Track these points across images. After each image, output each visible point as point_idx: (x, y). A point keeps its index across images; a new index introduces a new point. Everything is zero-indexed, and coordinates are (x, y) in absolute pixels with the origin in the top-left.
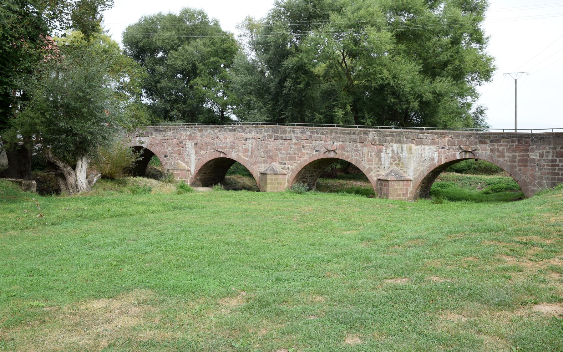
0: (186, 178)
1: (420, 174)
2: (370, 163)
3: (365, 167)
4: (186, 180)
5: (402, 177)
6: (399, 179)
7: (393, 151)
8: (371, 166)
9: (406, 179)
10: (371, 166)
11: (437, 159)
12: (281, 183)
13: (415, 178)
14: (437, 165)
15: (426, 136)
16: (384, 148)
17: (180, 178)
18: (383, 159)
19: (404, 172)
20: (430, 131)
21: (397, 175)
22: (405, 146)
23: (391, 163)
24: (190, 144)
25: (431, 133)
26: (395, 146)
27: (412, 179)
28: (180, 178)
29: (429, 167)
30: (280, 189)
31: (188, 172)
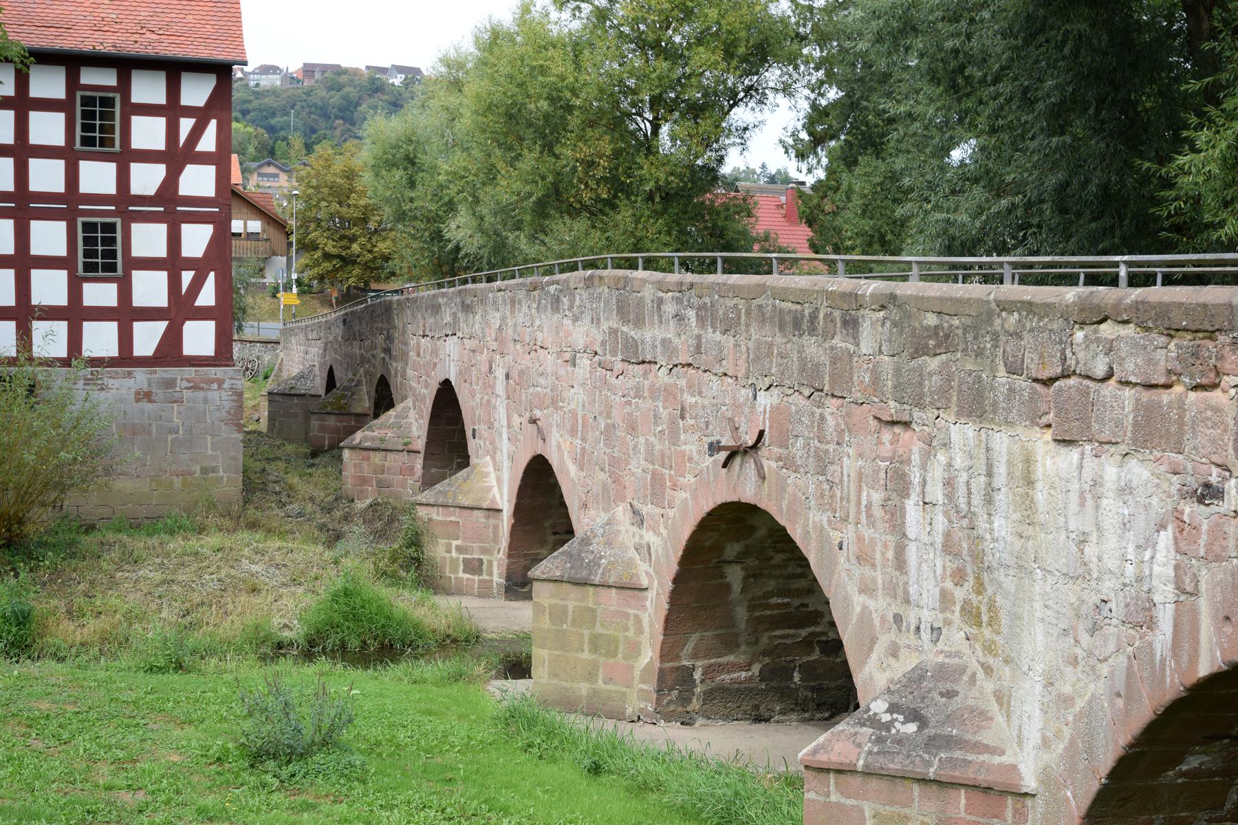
0: (484, 551)
1: (1072, 742)
2: (867, 571)
3: (847, 599)
4: (485, 558)
5: (950, 742)
6: (894, 766)
7: (949, 483)
8: (871, 604)
9: (970, 775)
10: (871, 604)
11: (1170, 608)
12: (615, 641)
13: (1046, 776)
14: (1173, 686)
15: (1110, 348)
16: (917, 448)
17: (459, 549)
18: (912, 552)
19: (999, 697)
20: (1158, 293)
21: (914, 716)
22: (1001, 441)
23: (946, 599)
24: (500, 373)
25: (1139, 317)
26: (962, 433)
27: (1030, 783)
28: (459, 549)
29: (1120, 686)
30: (608, 680)
31: (492, 521)
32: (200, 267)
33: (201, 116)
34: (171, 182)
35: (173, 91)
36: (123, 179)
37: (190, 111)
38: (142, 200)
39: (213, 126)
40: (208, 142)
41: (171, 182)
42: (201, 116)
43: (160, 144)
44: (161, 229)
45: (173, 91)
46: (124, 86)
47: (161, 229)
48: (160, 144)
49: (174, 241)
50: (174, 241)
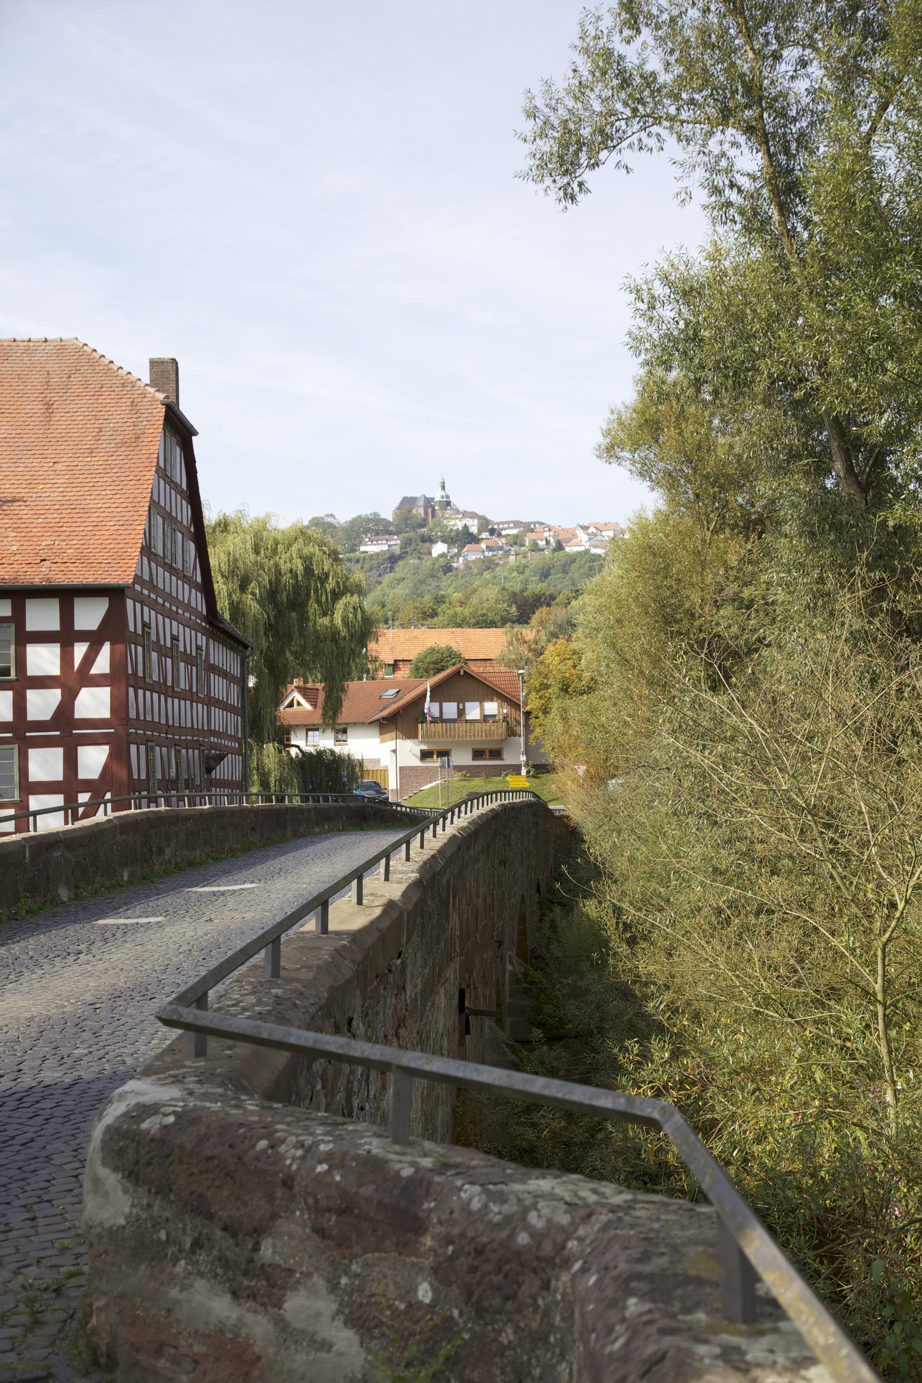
32: (94, 787)
33: (95, 639)
34: (66, 707)
35: (67, 617)
36: (20, 706)
37: (83, 636)
38: (39, 725)
39: (106, 649)
40: (102, 664)
41: (66, 707)
42: (95, 639)
43: (55, 670)
44: (59, 752)
45: (67, 617)
46: (19, 617)
47: (59, 752)
48: (55, 670)
49: (71, 762)
50: (71, 762)
